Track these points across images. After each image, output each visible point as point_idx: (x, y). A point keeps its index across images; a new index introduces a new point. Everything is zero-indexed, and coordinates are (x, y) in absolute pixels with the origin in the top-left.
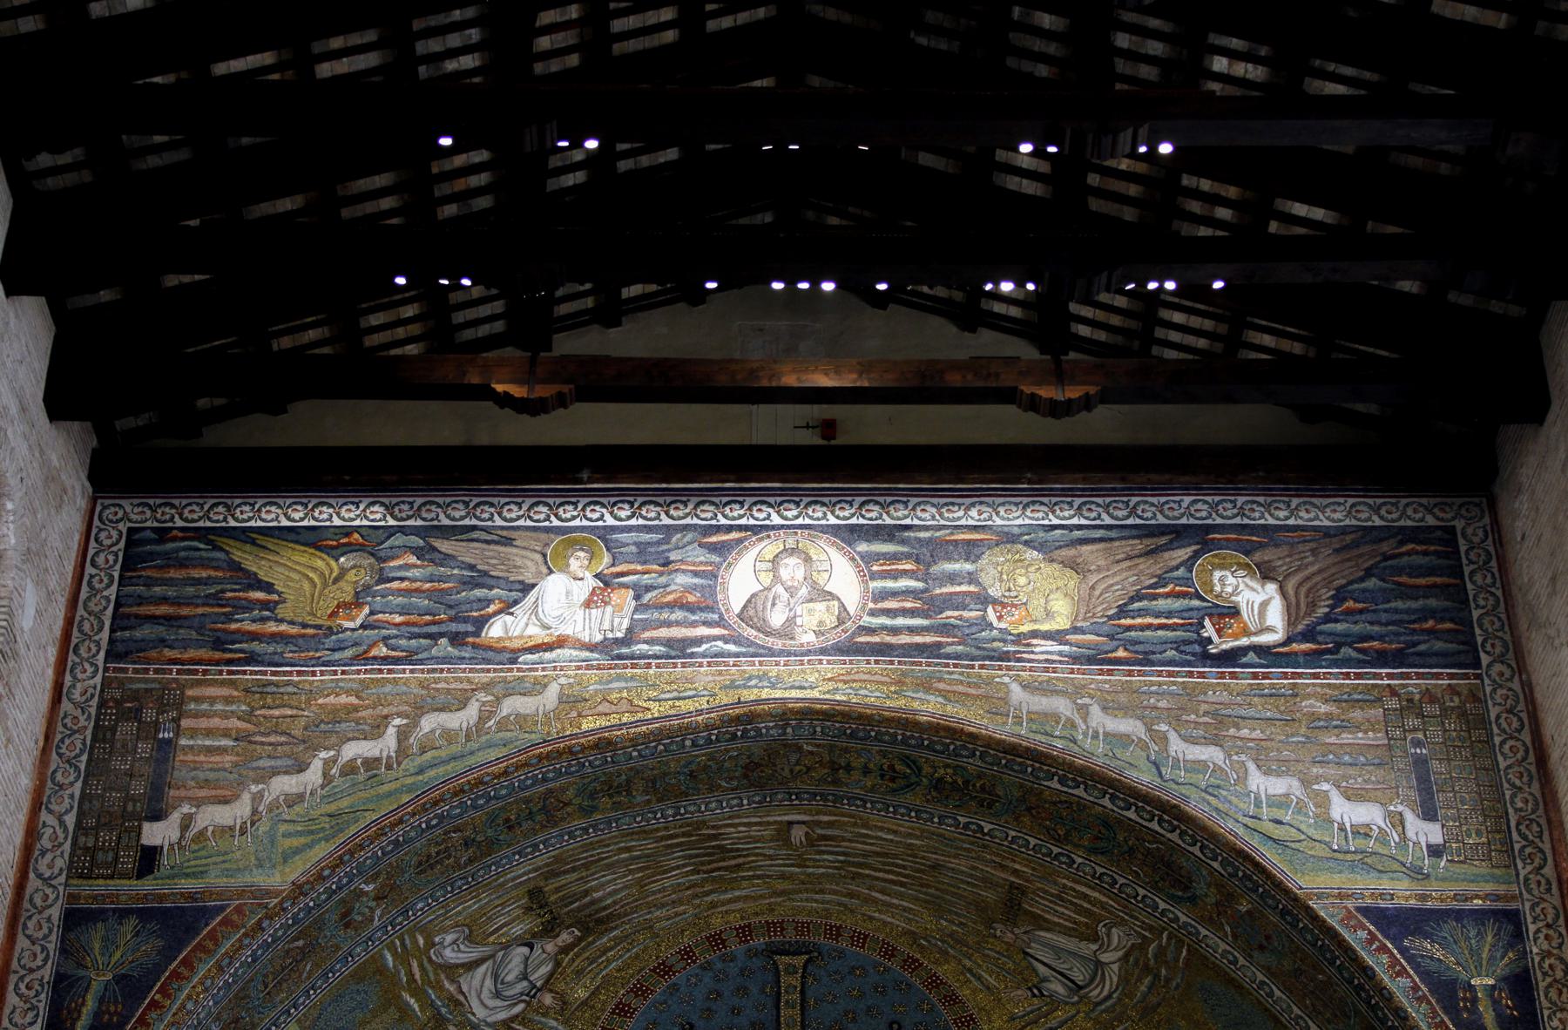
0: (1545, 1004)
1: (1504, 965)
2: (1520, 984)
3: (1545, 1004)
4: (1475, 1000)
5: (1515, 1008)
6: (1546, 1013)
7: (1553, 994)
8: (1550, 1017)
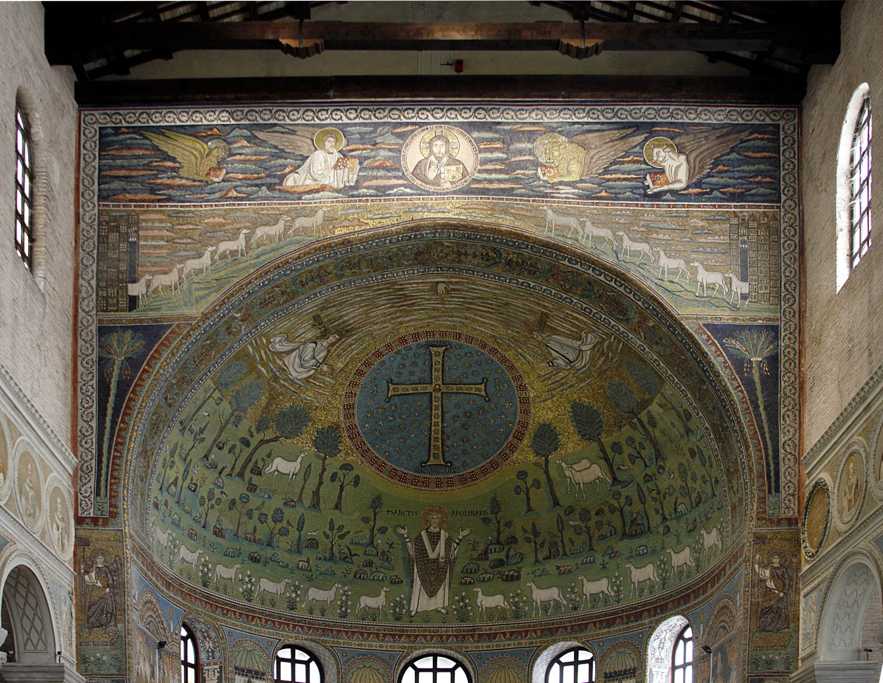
0: (783, 369)
1: (766, 353)
2: (773, 360)
3: (783, 369)
4: (751, 368)
6: (782, 374)
7: (787, 365)
8: (784, 376)
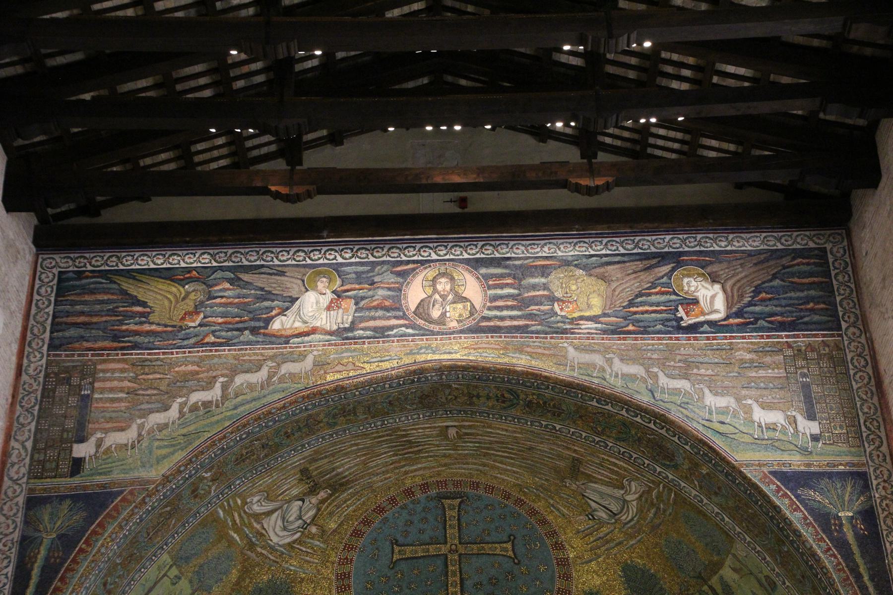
0: (884, 527)
1: (857, 505)
2: (868, 515)
3: (884, 527)
4: (841, 525)
5: (866, 529)
6: (885, 533)
8: (887, 535)
